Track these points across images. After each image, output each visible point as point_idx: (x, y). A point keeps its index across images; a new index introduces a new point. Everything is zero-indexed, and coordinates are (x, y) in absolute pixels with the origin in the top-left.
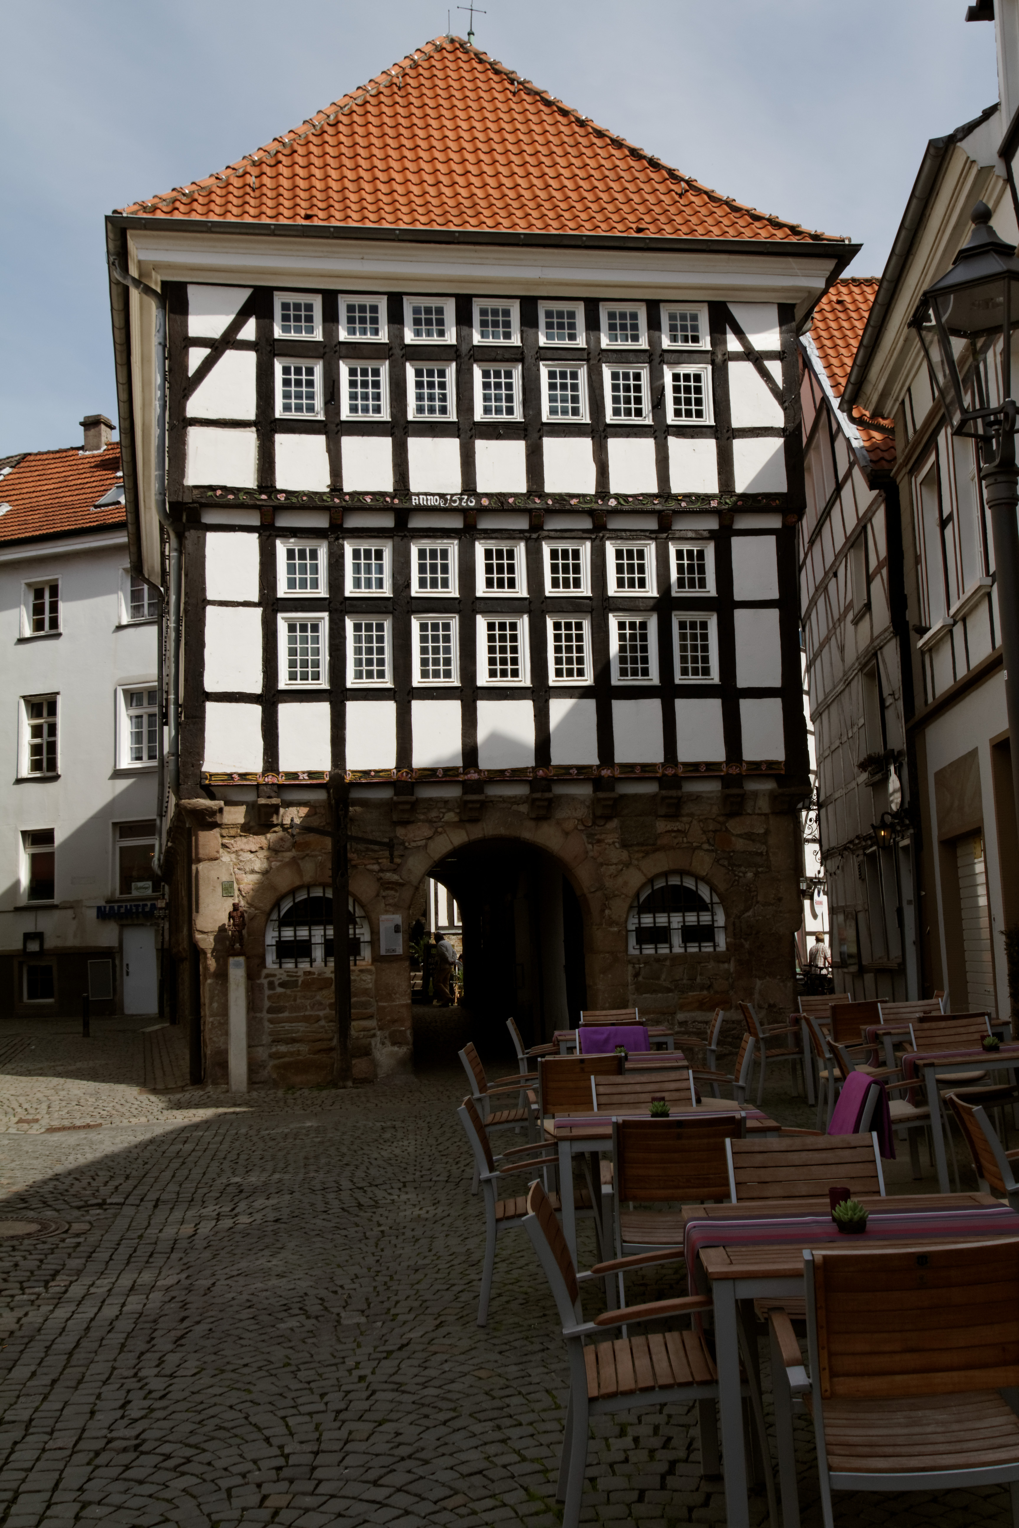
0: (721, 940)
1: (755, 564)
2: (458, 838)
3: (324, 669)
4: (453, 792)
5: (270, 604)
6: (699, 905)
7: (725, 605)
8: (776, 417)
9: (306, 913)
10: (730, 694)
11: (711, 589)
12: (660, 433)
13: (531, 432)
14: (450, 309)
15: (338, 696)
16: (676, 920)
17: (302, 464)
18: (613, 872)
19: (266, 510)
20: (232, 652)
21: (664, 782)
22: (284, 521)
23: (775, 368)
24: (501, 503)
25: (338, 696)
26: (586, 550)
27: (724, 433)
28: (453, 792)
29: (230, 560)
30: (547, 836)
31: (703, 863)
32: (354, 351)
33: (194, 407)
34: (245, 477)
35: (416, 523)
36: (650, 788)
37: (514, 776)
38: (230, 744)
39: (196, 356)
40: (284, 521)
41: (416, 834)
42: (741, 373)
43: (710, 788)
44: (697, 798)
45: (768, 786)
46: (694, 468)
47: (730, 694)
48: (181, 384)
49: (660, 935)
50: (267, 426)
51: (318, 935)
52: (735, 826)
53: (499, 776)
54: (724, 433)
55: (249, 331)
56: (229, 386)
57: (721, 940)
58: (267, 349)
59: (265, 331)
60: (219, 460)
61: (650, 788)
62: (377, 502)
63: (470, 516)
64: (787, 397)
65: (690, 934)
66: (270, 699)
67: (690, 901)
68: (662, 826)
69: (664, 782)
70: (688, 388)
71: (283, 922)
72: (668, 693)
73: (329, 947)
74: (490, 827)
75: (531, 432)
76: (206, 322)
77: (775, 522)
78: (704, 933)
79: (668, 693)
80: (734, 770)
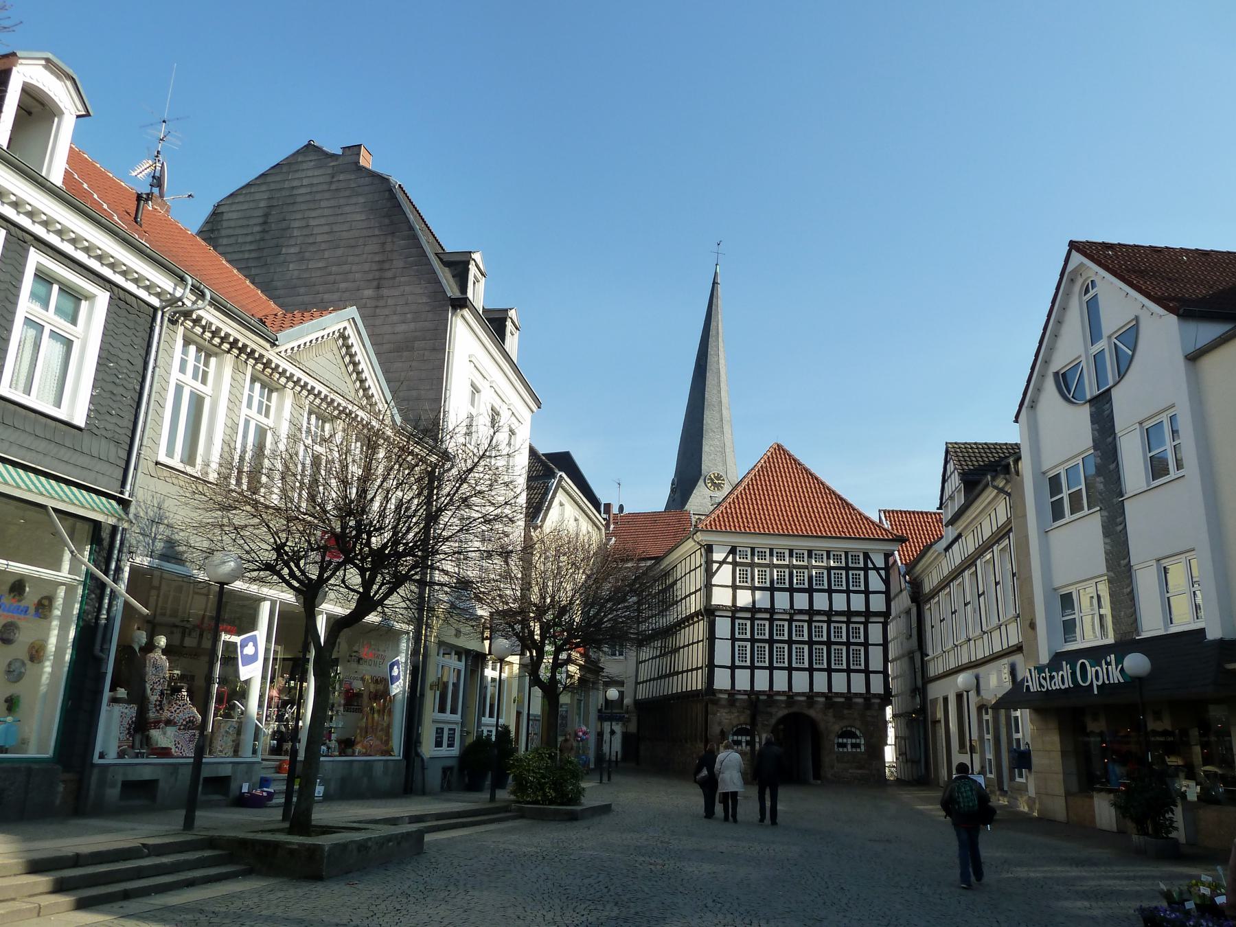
0: (863, 748)
1: (875, 632)
2: (786, 712)
3: (748, 659)
4: (783, 698)
5: (733, 639)
6: (857, 737)
7: (866, 644)
8: (883, 588)
9: (740, 732)
10: (867, 672)
11: (862, 640)
12: (848, 592)
13: (810, 591)
14: (787, 553)
15: (752, 668)
16: (849, 741)
17: (744, 599)
18: (831, 725)
19: (734, 610)
20: (723, 653)
21: (847, 698)
22: (738, 615)
23: (883, 573)
24: (801, 612)
25: (752, 668)
26: (825, 626)
27: (867, 592)
28: (783, 698)
29: (723, 627)
30: (812, 713)
31: (858, 723)
32: (759, 565)
33: (715, 581)
34: (728, 602)
35: (776, 617)
36: (842, 700)
37: (803, 694)
38: (722, 680)
39: (715, 566)
40: (738, 615)
41: (774, 710)
42: (872, 574)
43: (860, 700)
44: (856, 704)
45: (877, 701)
46: (858, 603)
47: (867, 672)
48: (710, 574)
49: (844, 745)
50: (734, 587)
51: (744, 739)
52: (869, 713)
53: (798, 694)
54: (867, 592)
55: (730, 559)
56: (724, 575)
57: (863, 748)
58: (735, 564)
59: (734, 559)
60: (721, 597)
61: (842, 700)
62: (766, 611)
63: (793, 613)
64: (887, 582)
65: (853, 745)
66: (733, 668)
67: (853, 735)
68: (846, 712)
69: (847, 698)
70: (856, 578)
71: (734, 734)
72: (849, 671)
73: (747, 743)
74: (794, 709)
75: (810, 591)
76: (718, 556)
77: (882, 620)
78: (858, 746)
79: (849, 671)
80: (868, 696)
